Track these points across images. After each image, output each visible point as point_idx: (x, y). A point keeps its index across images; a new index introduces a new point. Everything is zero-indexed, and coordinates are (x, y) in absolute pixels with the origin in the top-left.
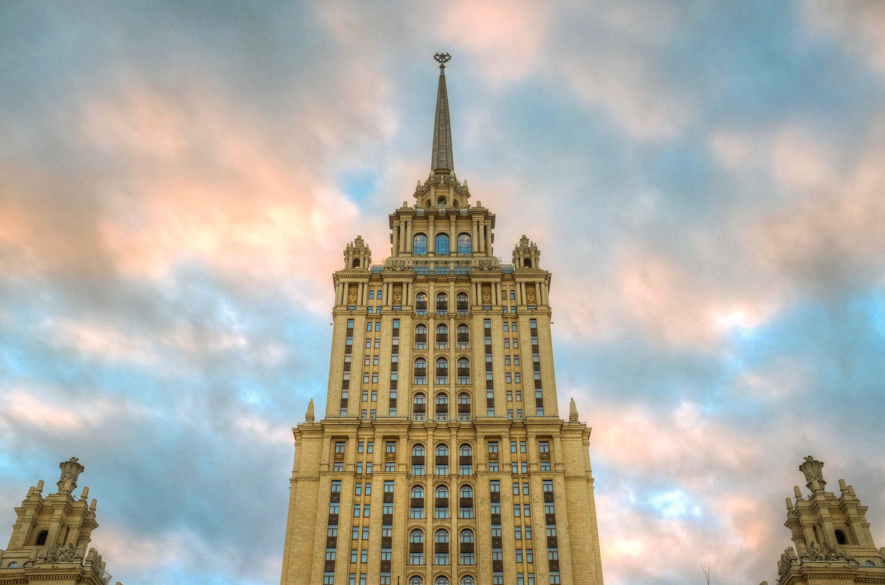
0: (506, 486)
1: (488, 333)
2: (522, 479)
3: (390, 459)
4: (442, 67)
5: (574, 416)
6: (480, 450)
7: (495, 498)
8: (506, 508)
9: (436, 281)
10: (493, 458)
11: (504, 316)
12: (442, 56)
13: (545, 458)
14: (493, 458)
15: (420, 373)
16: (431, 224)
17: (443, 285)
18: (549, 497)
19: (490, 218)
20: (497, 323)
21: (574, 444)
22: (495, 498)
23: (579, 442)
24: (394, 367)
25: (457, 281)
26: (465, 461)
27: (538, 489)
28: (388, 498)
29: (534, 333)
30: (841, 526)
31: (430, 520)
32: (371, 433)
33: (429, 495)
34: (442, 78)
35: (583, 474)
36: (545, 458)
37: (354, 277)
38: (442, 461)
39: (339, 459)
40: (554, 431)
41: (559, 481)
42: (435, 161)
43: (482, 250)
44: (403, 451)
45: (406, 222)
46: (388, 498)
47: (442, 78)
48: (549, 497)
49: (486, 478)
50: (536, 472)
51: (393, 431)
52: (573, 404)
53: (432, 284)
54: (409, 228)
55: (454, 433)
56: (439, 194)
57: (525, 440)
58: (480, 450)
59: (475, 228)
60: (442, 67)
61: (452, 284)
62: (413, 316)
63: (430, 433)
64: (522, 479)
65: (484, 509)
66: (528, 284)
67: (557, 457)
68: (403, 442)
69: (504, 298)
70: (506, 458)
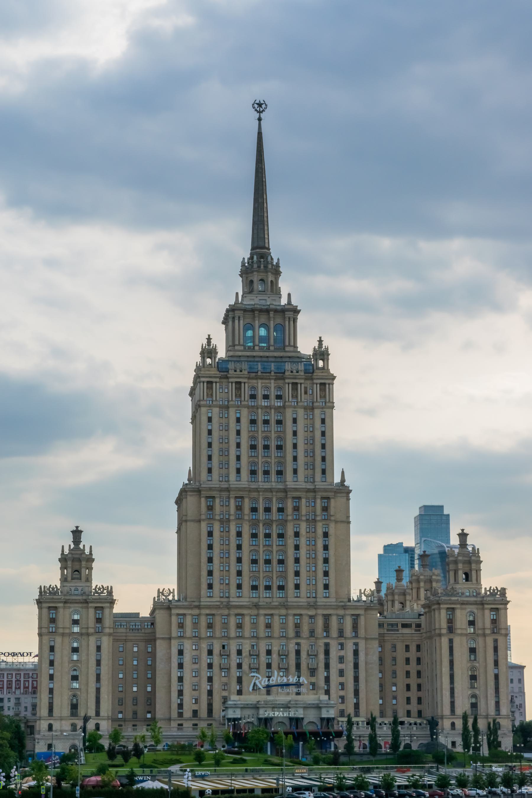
0: (303, 528)
1: (295, 421)
2: (312, 522)
3: (239, 508)
4: (260, 119)
5: (343, 480)
6: (290, 505)
7: (297, 534)
8: (303, 541)
9: (262, 379)
10: (296, 509)
11: (305, 408)
12: (260, 105)
13: (325, 509)
14: (296, 509)
15: (253, 447)
16: (257, 319)
17: (267, 381)
18: (326, 535)
19: (296, 311)
20: (301, 413)
21: (341, 500)
22: (297, 534)
23: (344, 499)
24: (238, 445)
25: (275, 379)
26: (281, 510)
27: (320, 532)
28: (239, 534)
29: (323, 421)
30: (467, 570)
31: (261, 546)
32: (228, 493)
33: (262, 531)
34: (260, 134)
35: (344, 519)
36: (325, 509)
37: (210, 377)
38: (268, 510)
39: (210, 508)
40: (330, 494)
41: (332, 525)
42: (255, 232)
43: (292, 344)
44: (247, 505)
45: (239, 317)
46: (239, 534)
47: (260, 134)
48: (326, 535)
49: (292, 524)
50: (319, 521)
51: (240, 494)
52: (343, 473)
53: (260, 381)
54: (241, 322)
55: (274, 494)
56: (260, 278)
57: (315, 498)
58: (290, 505)
59: (287, 323)
60: (260, 119)
61: (272, 381)
62: (248, 407)
63: (261, 494)
64: (312, 522)
65: (291, 541)
66: (321, 384)
67: (332, 511)
68: (246, 500)
69: (306, 393)
70: (304, 510)
